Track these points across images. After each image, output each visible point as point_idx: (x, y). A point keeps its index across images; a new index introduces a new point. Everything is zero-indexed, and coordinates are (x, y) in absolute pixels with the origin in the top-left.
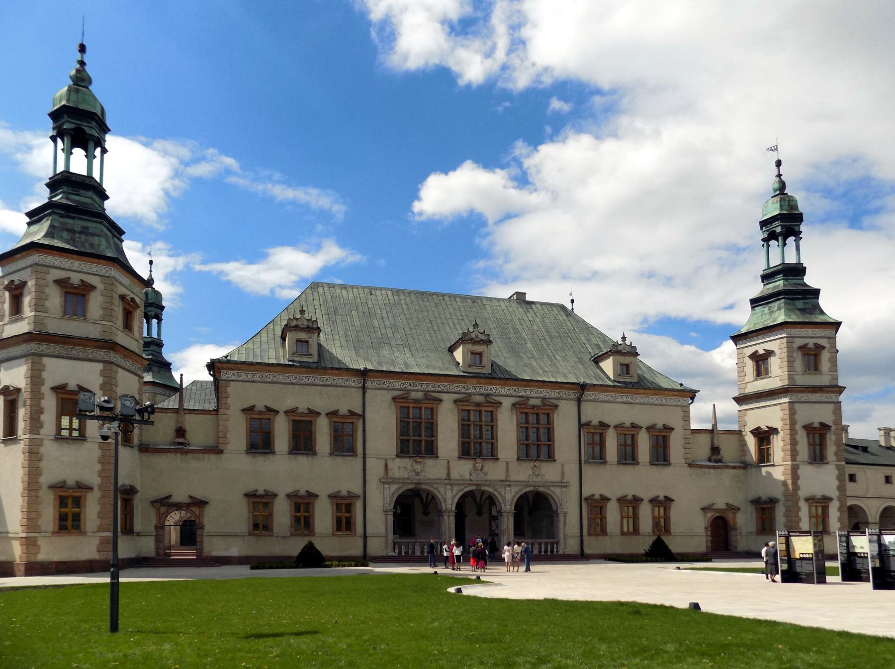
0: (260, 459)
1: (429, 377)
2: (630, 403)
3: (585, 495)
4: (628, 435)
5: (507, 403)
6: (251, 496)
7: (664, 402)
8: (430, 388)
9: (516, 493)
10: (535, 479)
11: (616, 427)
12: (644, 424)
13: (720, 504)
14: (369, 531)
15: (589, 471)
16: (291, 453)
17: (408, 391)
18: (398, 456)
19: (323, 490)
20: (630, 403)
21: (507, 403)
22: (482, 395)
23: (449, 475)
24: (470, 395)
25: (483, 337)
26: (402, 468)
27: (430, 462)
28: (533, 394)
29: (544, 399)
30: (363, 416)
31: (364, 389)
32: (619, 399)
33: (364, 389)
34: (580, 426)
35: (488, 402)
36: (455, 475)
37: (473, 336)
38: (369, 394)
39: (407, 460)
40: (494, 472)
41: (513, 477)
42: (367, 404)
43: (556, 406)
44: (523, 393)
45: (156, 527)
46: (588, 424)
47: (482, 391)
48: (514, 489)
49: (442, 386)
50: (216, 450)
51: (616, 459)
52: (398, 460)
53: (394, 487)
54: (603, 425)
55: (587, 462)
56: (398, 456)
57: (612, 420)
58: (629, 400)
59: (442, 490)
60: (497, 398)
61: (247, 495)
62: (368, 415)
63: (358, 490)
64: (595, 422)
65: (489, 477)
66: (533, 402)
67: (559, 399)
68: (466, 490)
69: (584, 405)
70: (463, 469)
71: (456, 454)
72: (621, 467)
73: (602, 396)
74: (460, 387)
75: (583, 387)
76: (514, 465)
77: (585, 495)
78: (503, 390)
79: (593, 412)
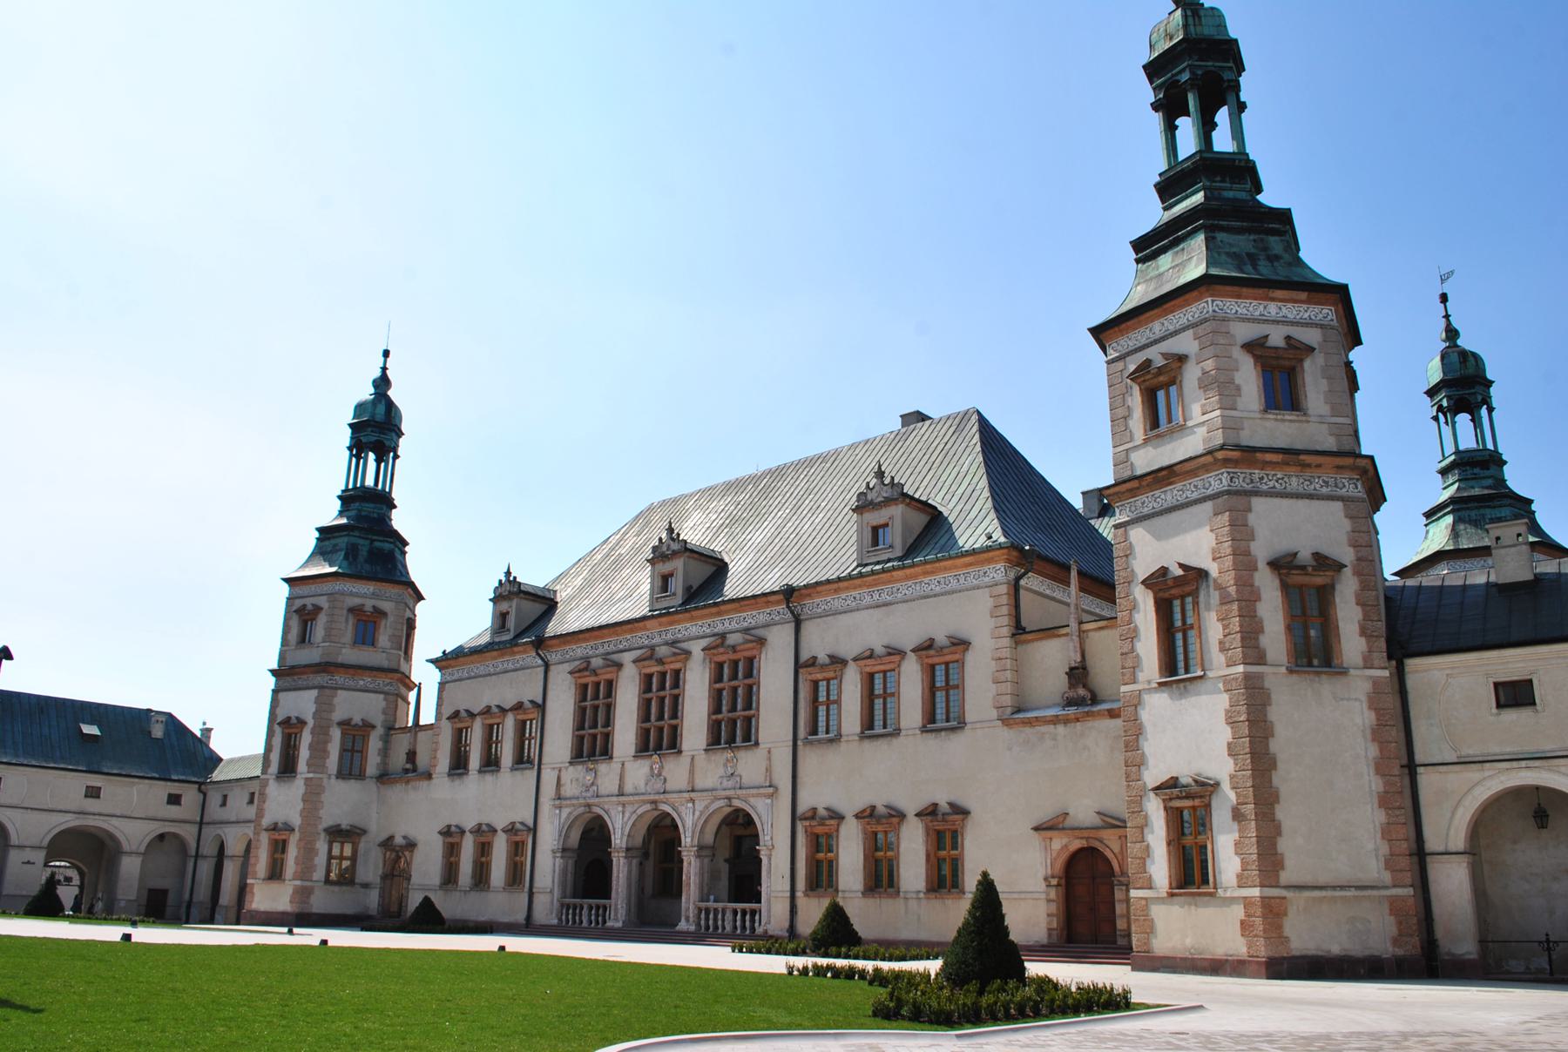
0: (457, 782)
1: (605, 631)
2: (886, 604)
3: (802, 808)
4: (878, 673)
5: (696, 648)
6: (446, 832)
7: (954, 584)
8: (612, 648)
9: (702, 813)
10: (726, 784)
11: (855, 659)
12: (908, 641)
13: (1084, 812)
14: (538, 883)
15: (809, 758)
16: (480, 772)
17: (587, 660)
18: (571, 763)
19: (500, 823)
20: (886, 604)
21: (696, 648)
22: (666, 644)
23: (621, 787)
24: (652, 648)
25: (675, 546)
26: (575, 778)
27: (603, 767)
28: (734, 626)
29: (746, 631)
30: (541, 707)
31: (547, 666)
32: (867, 600)
33: (547, 666)
34: (798, 666)
35: (675, 654)
36: (629, 788)
37: (664, 548)
38: (553, 670)
39: (580, 767)
40: (676, 771)
41: (699, 784)
42: (550, 686)
43: (761, 642)
44: (720, 628)
45: (384, 877)
46: (813, 662)
47: (670, 637)
48: (700, 806)
49: (626, 639)
50: (429, 776)
51: (858, 729)
52: (571, 768)
53: (565, 812)
54: (837, 662)
55: (807, 742)
56: (571, 763)
57: (848, 649)
58: (886, 597)
59: (613, 813)
60: (684, 645)
61: (440, 833)
62: (549, 704)
63: (530, 823)
64: (822, 658)
65: (669, 787)
66: (733, 639)
67: (767, 626)
68: (640, 812)
69: (811, 630)
70: (638, 773)
71: (632, 750)
72: (867, 744)
73: (836, 602)
74: (641, 638)
75: (789, 593)
76: (701, 757)
77: (802, 808)
78: (693, 629)
79: (818, 642)
